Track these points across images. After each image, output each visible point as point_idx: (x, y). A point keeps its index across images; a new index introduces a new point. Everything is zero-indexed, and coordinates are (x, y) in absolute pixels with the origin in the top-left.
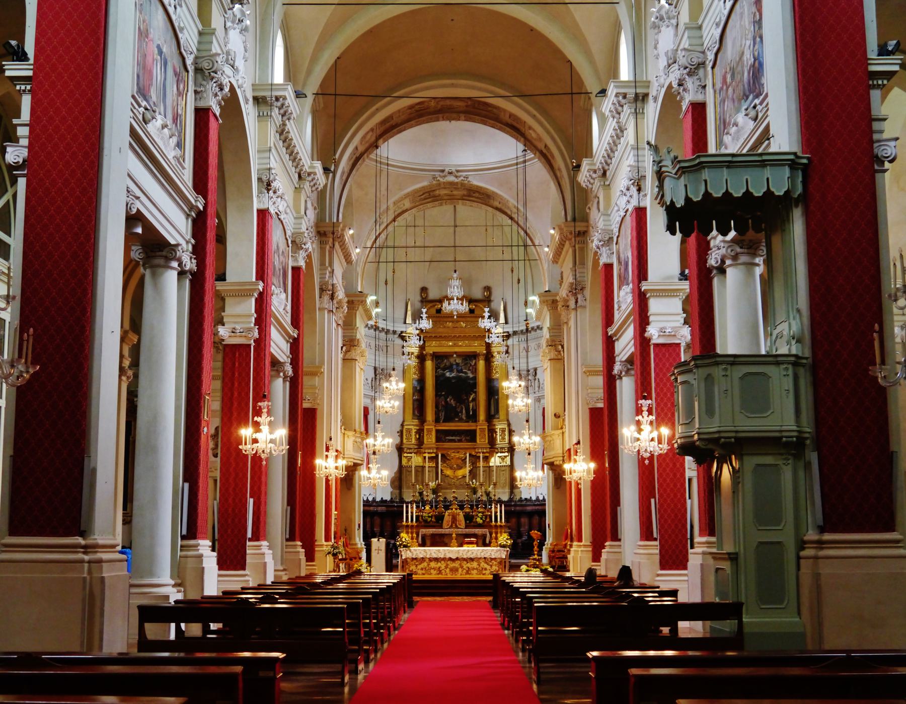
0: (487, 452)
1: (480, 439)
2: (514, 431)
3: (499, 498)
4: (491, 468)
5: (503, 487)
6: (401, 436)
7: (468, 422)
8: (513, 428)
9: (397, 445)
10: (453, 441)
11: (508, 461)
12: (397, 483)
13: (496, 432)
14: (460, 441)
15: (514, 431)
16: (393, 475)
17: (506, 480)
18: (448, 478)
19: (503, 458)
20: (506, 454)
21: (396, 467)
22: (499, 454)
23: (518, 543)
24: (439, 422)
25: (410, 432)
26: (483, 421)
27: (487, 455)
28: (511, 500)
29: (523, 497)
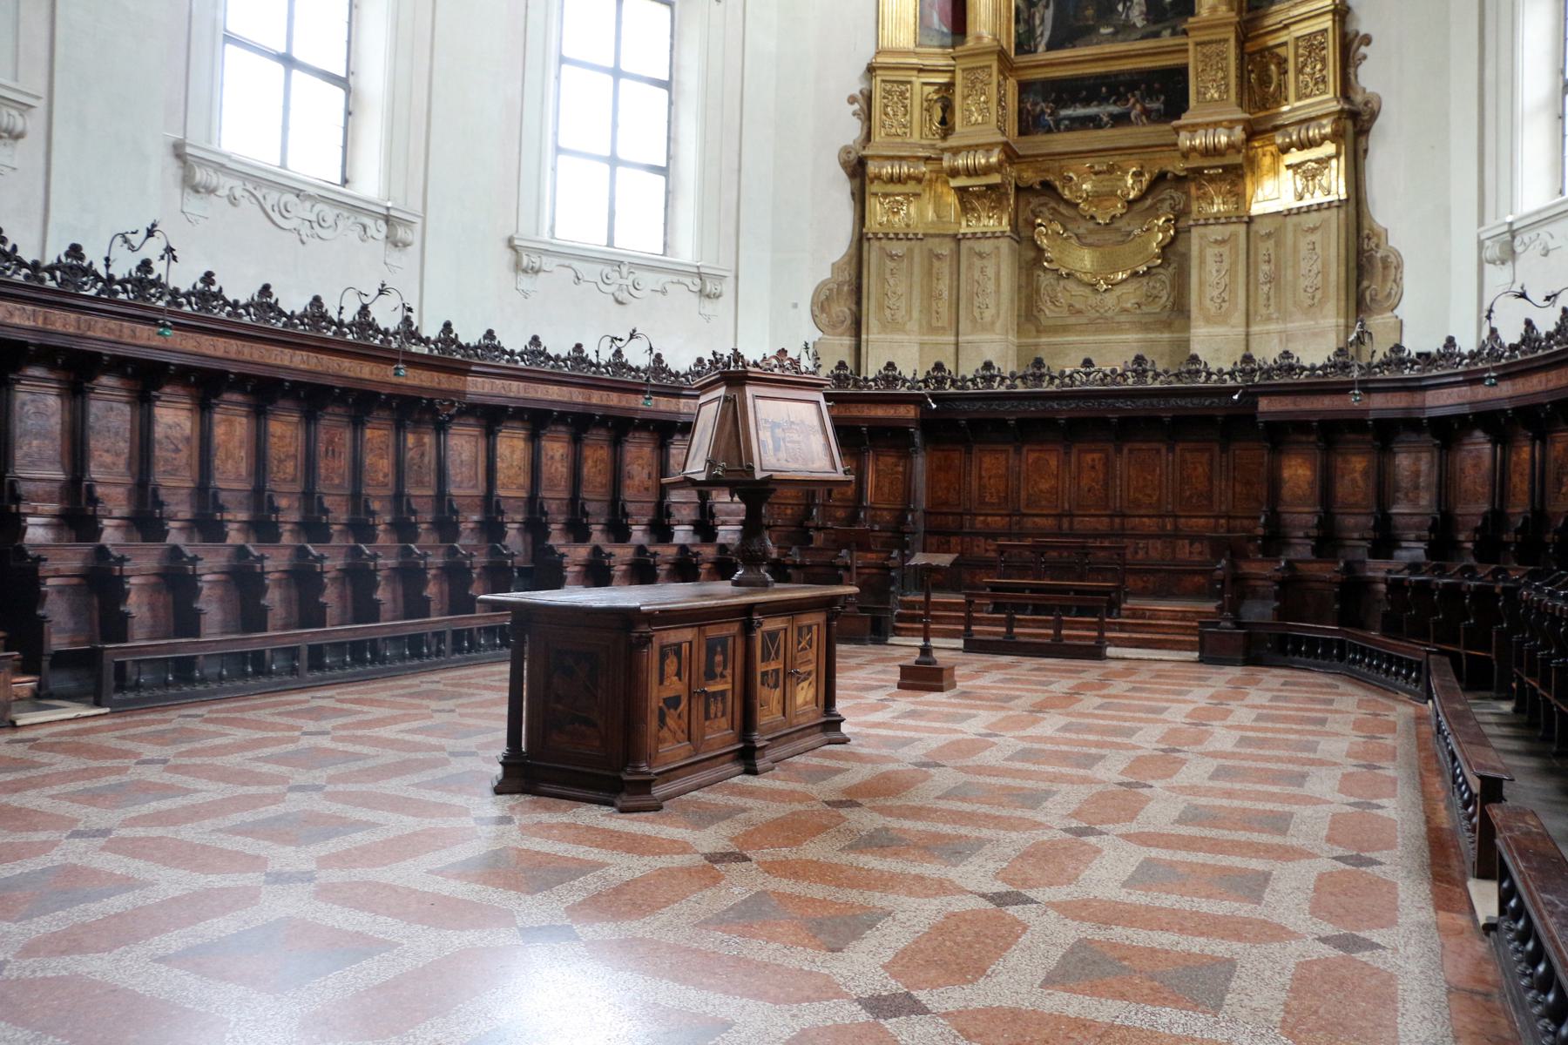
0: (1230, 146)
1: (1198, 93)
2: (1367, 40)
3: (1286, 354)
4: (1254, 227)
5: (1312, 308)
6: (867, 115)
7: (1156, 35)
8: (1363, 24)
9: (846, 150)
10: (1094, 122)
11: (1334, 184)
12: (843, 309)
13: (1281, 63)
14: (1120, 120)
15: (1367, 40)
16: (827, 275)
17: (1324, 272)
18: (1071, 285)
19: (1310, 173)
20: (1329, 148)
21: (840, 243)
22: (1295, 156)
23: (1373, 581)
24: (1035, 51)
25: (902, 94)
26: (1214, 9)
27: (1239, 159)
28: (1343, 360)
29: (1417, 341)
